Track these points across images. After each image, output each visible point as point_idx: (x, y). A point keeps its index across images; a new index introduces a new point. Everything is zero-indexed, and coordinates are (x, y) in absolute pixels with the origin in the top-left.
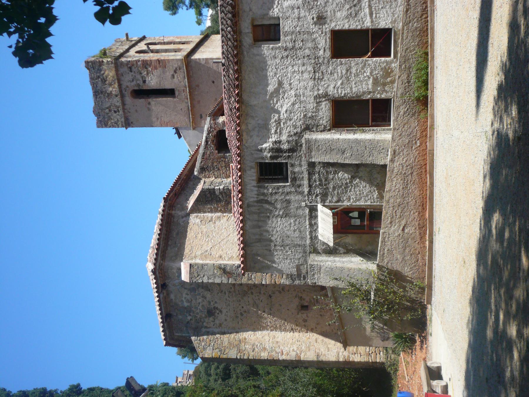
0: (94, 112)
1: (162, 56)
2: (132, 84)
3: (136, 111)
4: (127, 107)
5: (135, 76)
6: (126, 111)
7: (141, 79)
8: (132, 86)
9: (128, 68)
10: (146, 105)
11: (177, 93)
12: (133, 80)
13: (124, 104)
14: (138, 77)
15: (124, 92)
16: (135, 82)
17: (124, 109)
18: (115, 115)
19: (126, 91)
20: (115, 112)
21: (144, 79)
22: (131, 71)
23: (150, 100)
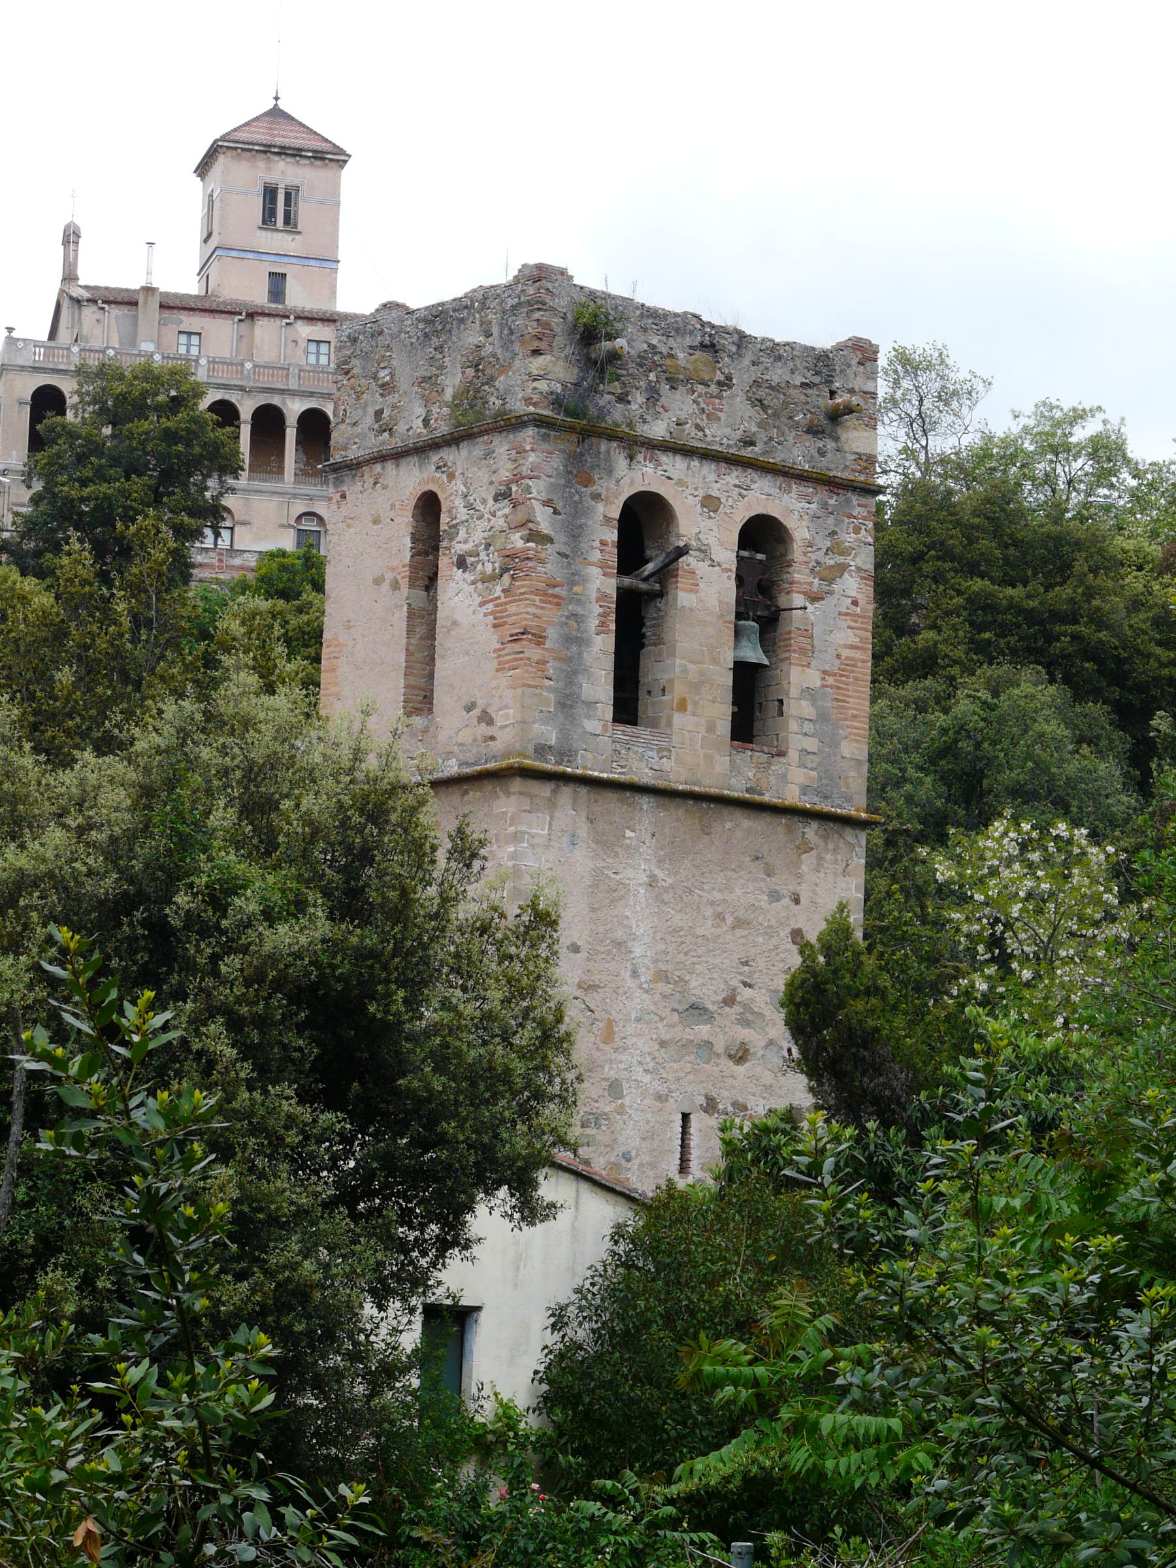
0: (385, 305)
1: (575, 640)
2: (459, 502)
3: (376, 521)
4: (390, 466)
5: (479, 518)
6: (378, 468)
7: (468, 546)
8: (454, 507)
9: (508, 484)
10: (393, 569)
11: (418, 721)
12: (470, 507)
13: (398, 455)
14: (478, 536)
15: (435, 458)
16: (462, 513)
17: (381, 458)
18: (371, 411)
19: (438, 468)
20: (379, 414)
21: (470, 560)
22: (497, 498)
23: (405, 590)
